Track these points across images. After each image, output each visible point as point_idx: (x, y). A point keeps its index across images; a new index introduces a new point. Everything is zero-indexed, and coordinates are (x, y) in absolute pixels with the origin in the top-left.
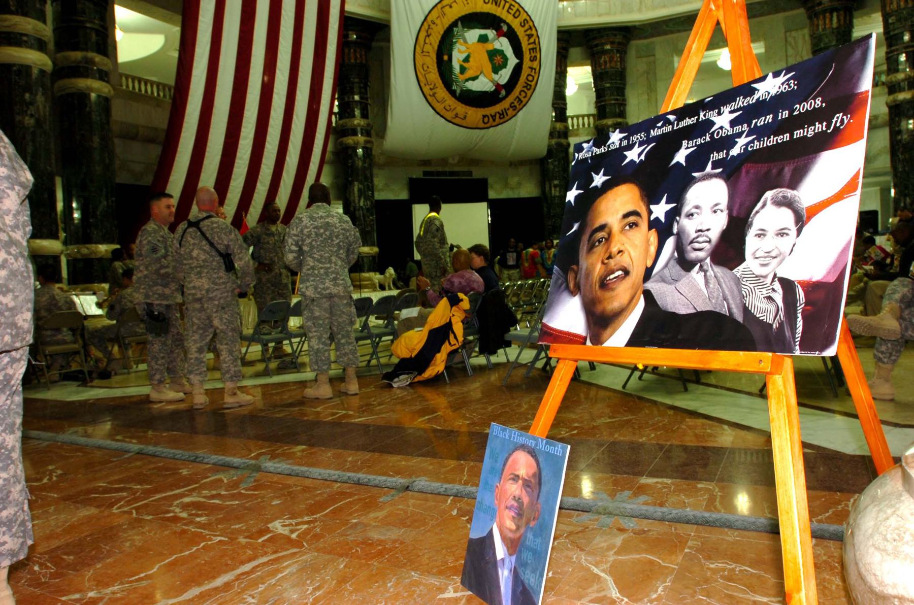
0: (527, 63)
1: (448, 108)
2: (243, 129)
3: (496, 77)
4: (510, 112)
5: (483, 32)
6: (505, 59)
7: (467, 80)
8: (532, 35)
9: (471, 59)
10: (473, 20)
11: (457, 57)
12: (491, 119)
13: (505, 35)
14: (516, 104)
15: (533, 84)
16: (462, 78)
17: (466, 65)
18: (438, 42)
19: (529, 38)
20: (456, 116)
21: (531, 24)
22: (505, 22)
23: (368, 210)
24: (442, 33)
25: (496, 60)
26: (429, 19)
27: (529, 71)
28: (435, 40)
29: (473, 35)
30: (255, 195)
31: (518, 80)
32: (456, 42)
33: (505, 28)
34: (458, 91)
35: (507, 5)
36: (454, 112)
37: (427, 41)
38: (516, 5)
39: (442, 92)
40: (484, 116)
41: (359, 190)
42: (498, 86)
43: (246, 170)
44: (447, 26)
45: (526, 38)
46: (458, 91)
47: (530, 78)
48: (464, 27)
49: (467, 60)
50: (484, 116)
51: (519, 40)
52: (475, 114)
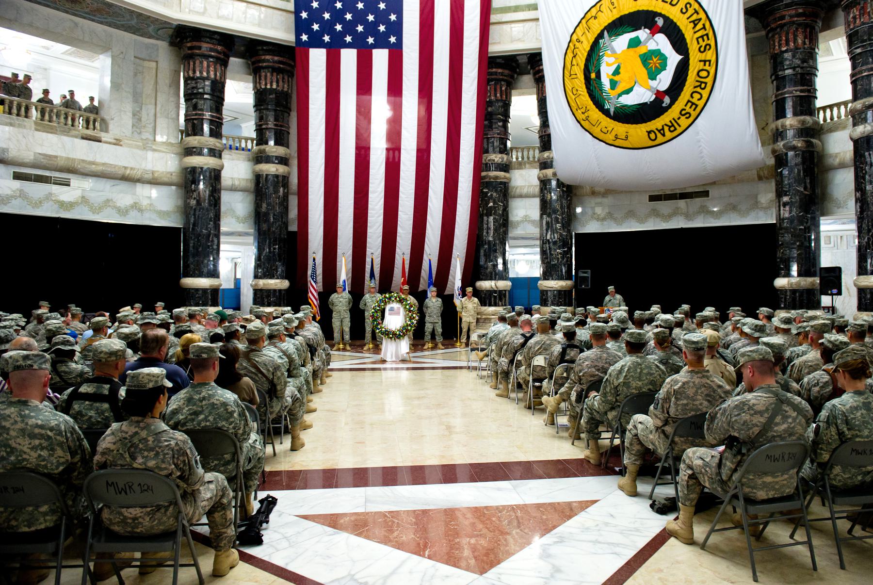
0: (695, 57)
1: (605, 130)
2: (370, 185)
3: (653, 84)
6: (663, 59)
7: (620, 95)
8: (700, 20)
10: (617, 27)
12: (659, 135)
13: (661, 30)
14: (688, 109)
15: (709, 80)
16: (613, 94)
17: (616, 78)
18: (584, 60)
19: (695, 25)
22: (660, 15)
23: (555, 243)
24: (588, 49)
25: (652, 63)
26: (575, 37)
28: (581, 60)
29: (621, 42)
30: (398, 238)
31: (685, 80)
33: (660, 22)
36: (614, 133)
37: (574, 63)
39: (595, 114)
40: (649, 133)
41: (547, 223)
42: (658, 93)
43: (382, 217)
44: (592, 40)
45: (692, 25)
47: (704, 74)
48: (610, 37)
49: (617, 72)
50: (649, 133)
51: (680, 30)
52: (638, 132)
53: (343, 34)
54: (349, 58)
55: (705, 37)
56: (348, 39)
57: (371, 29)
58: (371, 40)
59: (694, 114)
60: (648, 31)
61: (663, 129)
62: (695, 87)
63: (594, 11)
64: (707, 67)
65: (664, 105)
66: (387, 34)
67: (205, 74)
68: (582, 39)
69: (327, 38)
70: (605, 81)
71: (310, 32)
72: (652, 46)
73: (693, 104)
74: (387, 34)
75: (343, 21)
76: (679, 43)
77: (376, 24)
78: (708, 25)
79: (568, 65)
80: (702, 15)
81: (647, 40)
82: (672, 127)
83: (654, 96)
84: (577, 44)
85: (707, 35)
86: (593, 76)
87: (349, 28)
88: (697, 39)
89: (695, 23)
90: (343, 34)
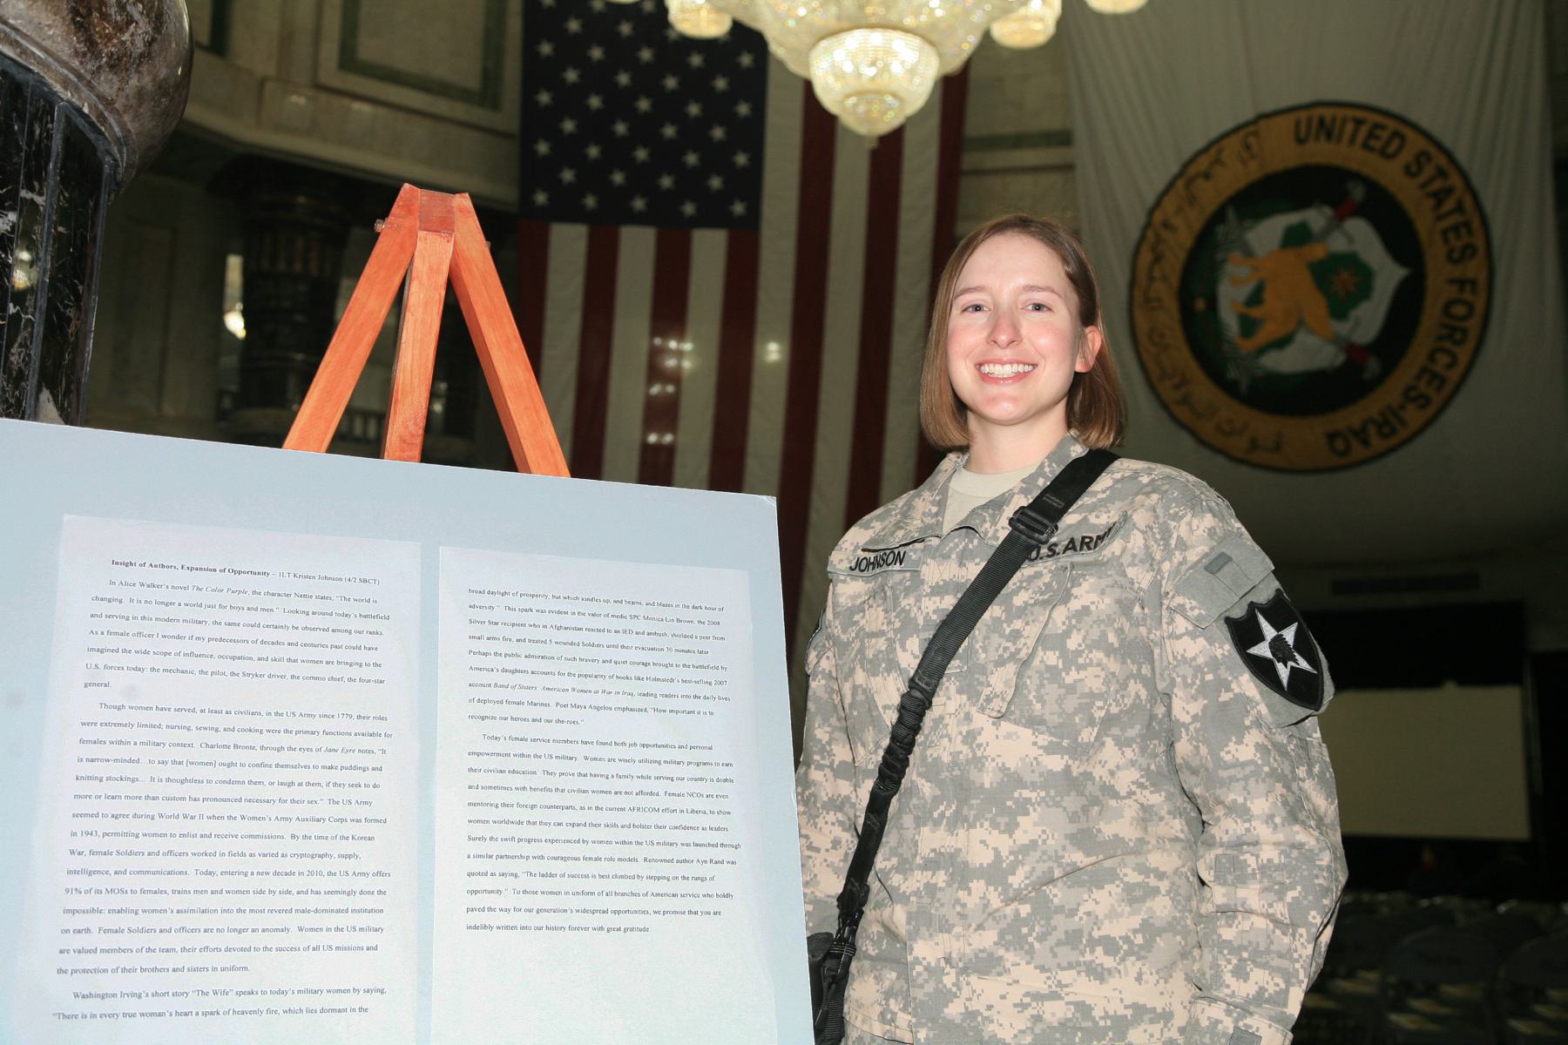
0: (1438, 272)
3: (1342, 328)
4: (1414, 416)
5: (1293, 218)
7: (1263, 350)
8: (1449, 191)
9: (1268, 296)
11: (1231, 296)
12: (1355, 444)
13: (1361, 211)
14: (1423, 387)
15: (1473, 325)
16: (1247, 346)
17: (1255, 312)
18: (1178, 267)
20: (1254, 445)
21: (1441, 160)
25: (1340, 282)
27: (1453, 292)
29: (1267, 233)
32: (1224, 261)
33: (1358, 192)
34: (1244, 384)
35: (1364, 130)
37: (1157, 273)
38: (1392, 125)
39: (1204, 390)
40: (1332, 437)
45: (1431, 202)
46: (1244, 384)
47: (1460, 310)
49: (1255, 298)
50: (1332, 437)
52: (1305, 434)
53: (627, 193)
54: (637, 247)
55: (1463, 231)
56: (639, 204)
57: (691, 184)
58: (689, 209)
59: (1437, 399)
60: (1328, 211)
61: (1364, 430)
62: (1441, 338)
63: (1203, 162)
64: (1467, 296)
65: (1367, 376)
66: (726, 197)
67: (298, 267)
68: (1178, 221)
69: (590, 202)
70: (1229, 318)
71: (554, 187)
72: (1337, 243)
73: (1434, 375)
74: (726, 197)
75: (628, 164)
76: (1399, 237)
77: (702, 172)
78: (1468, 203)
79: (1142, 277)
80: (1456, 181)
81: (1327, 231)
82: (1387, 423)
83: (1341, 359)
84: (1166, 234)
85: (1467, 225)
86: (1200, 305)
87: (642, 179)
88: (1444, 233)
89: (1439, 197)
90: (627, 193)
